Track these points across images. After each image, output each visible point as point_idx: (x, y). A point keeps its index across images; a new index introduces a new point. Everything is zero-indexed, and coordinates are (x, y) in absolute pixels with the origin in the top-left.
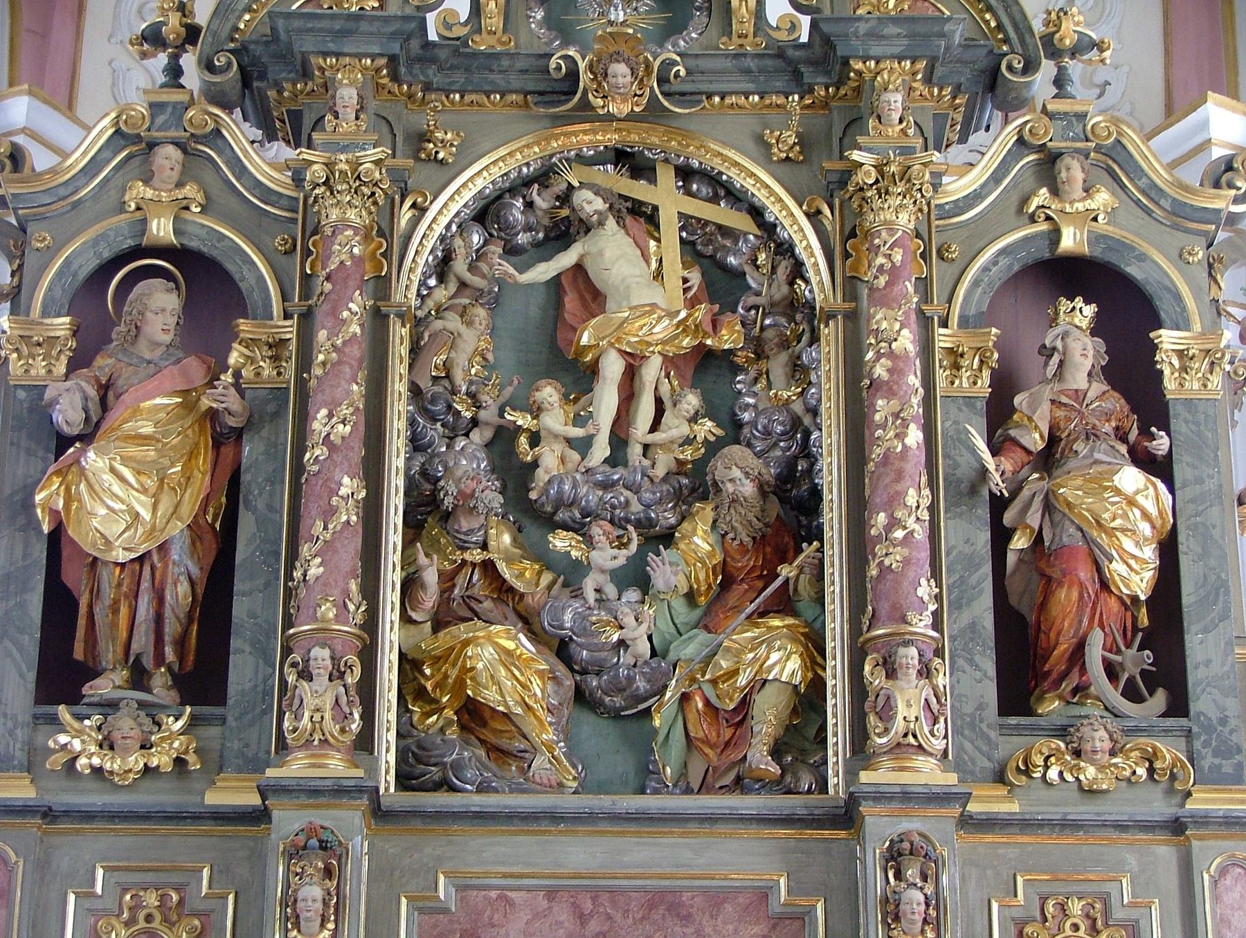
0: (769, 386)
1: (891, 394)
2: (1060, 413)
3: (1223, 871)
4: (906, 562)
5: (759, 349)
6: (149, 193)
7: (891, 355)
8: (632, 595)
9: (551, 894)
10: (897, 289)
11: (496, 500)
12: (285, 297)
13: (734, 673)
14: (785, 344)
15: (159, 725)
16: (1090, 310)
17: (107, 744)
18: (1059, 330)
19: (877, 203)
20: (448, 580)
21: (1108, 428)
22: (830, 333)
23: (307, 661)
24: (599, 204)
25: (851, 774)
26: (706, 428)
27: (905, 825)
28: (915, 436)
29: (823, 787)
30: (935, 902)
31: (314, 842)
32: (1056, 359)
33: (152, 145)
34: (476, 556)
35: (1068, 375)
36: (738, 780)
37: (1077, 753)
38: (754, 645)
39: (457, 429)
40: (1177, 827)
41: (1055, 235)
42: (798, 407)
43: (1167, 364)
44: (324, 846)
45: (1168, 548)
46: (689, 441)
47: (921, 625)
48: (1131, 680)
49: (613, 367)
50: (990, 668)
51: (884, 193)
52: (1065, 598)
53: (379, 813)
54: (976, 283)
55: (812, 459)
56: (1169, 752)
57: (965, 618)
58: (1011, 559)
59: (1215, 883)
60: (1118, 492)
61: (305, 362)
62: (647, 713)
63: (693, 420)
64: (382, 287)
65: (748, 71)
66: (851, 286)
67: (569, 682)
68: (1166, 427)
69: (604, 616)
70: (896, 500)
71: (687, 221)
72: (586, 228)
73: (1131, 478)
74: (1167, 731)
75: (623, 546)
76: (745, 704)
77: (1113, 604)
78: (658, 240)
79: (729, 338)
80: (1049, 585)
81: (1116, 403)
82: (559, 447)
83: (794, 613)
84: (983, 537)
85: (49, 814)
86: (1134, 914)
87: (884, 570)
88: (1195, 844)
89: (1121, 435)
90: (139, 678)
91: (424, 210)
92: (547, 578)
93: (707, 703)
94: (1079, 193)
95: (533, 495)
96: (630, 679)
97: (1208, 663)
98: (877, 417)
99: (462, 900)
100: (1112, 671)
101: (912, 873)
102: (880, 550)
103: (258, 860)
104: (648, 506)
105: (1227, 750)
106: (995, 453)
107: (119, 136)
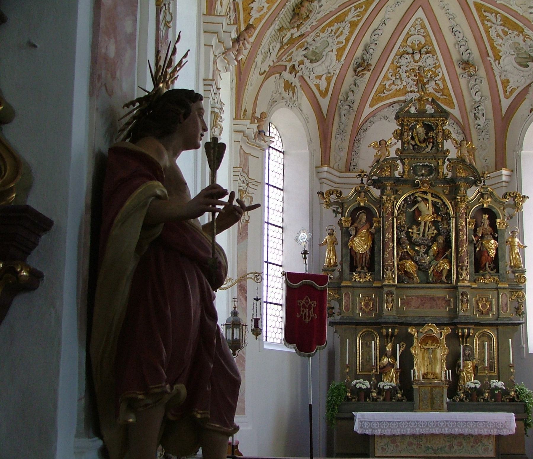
0: (444, 225)
1: (462, 231)
2: (483, 231)
3: (503, 294)
4: (464, 255)
5: (442, 219)
6: (360, 199)
7: (462, 226)
8: (426, 255)
9: (418, 297)
10: (463, 216)
11: (408, 242)
12: (380, 215)
13: (440, 267)
14: (446, 219)
15: (366, 275)
16: (487, 216)
17: (360, 278)
18: (483, 219)
19: (460, 204)
20: (402, 253)
21: (489, 233)
22: (453, 220)
23: (387, 268)
24: (421, 199)
26: (435, 232)
27: (464, 290)
28: (465, 237)
29: (452, 283)
30: (467, 300)
31: (390, 293)
32: (483, 224)
34: (405, 250)
35: (484, 226)
36: (441, 281)
37: (485, 279)
40: (497, 289)
41: (483, 205)
42: (448, 228)
43: (498, 224)
44: (391, 293)
45: (497, 250)
46: (433, 233)
48: (492, 268)
49: (423, 223)
51: (461, 202)
52: (484, 258)
53: (397, 287)
54: (472, 212)
55: (450, 236)
56: (496, 278)
57: (471, 259)
58: (476, 251)
59: (501, 296)
60: (491, 243)
62: (428, 271)
63: (434, 230)
65: (442, 182)
67: (418, 267)
68: (497, 233)
69: (422, 258)
70: (462, 246)
71: (432, 201)
72: (419, 202)
73: (493, 241)
74: (495, 275)
75: (424, 248)
76: (442, 271)
77: (490, 258)
78: (428, 204)
79: (439, 219)
80: (482, 256)
81: (491, 229)
82: (416, 234)
83: (448, 259)
84: (473, 248)
85: (354, 287)
86: (491, 300)
87: (461, 256)
88: (499, 291)
89: (491, 234)
90: (362, 268)
91: (398, 202)
92: (414, 253)
93: (436, 270)
94: (486, 199)
95: (412, 241)
96: (426, 267)
97: (501, 266)
98: (460, 235)
99: (407, 298)
100: (489, 267)
101: (464, 296)
102: (460, 253)
103: (381, 293)
104: (428, 243)
105: (504, 278)
106: (475, 237)
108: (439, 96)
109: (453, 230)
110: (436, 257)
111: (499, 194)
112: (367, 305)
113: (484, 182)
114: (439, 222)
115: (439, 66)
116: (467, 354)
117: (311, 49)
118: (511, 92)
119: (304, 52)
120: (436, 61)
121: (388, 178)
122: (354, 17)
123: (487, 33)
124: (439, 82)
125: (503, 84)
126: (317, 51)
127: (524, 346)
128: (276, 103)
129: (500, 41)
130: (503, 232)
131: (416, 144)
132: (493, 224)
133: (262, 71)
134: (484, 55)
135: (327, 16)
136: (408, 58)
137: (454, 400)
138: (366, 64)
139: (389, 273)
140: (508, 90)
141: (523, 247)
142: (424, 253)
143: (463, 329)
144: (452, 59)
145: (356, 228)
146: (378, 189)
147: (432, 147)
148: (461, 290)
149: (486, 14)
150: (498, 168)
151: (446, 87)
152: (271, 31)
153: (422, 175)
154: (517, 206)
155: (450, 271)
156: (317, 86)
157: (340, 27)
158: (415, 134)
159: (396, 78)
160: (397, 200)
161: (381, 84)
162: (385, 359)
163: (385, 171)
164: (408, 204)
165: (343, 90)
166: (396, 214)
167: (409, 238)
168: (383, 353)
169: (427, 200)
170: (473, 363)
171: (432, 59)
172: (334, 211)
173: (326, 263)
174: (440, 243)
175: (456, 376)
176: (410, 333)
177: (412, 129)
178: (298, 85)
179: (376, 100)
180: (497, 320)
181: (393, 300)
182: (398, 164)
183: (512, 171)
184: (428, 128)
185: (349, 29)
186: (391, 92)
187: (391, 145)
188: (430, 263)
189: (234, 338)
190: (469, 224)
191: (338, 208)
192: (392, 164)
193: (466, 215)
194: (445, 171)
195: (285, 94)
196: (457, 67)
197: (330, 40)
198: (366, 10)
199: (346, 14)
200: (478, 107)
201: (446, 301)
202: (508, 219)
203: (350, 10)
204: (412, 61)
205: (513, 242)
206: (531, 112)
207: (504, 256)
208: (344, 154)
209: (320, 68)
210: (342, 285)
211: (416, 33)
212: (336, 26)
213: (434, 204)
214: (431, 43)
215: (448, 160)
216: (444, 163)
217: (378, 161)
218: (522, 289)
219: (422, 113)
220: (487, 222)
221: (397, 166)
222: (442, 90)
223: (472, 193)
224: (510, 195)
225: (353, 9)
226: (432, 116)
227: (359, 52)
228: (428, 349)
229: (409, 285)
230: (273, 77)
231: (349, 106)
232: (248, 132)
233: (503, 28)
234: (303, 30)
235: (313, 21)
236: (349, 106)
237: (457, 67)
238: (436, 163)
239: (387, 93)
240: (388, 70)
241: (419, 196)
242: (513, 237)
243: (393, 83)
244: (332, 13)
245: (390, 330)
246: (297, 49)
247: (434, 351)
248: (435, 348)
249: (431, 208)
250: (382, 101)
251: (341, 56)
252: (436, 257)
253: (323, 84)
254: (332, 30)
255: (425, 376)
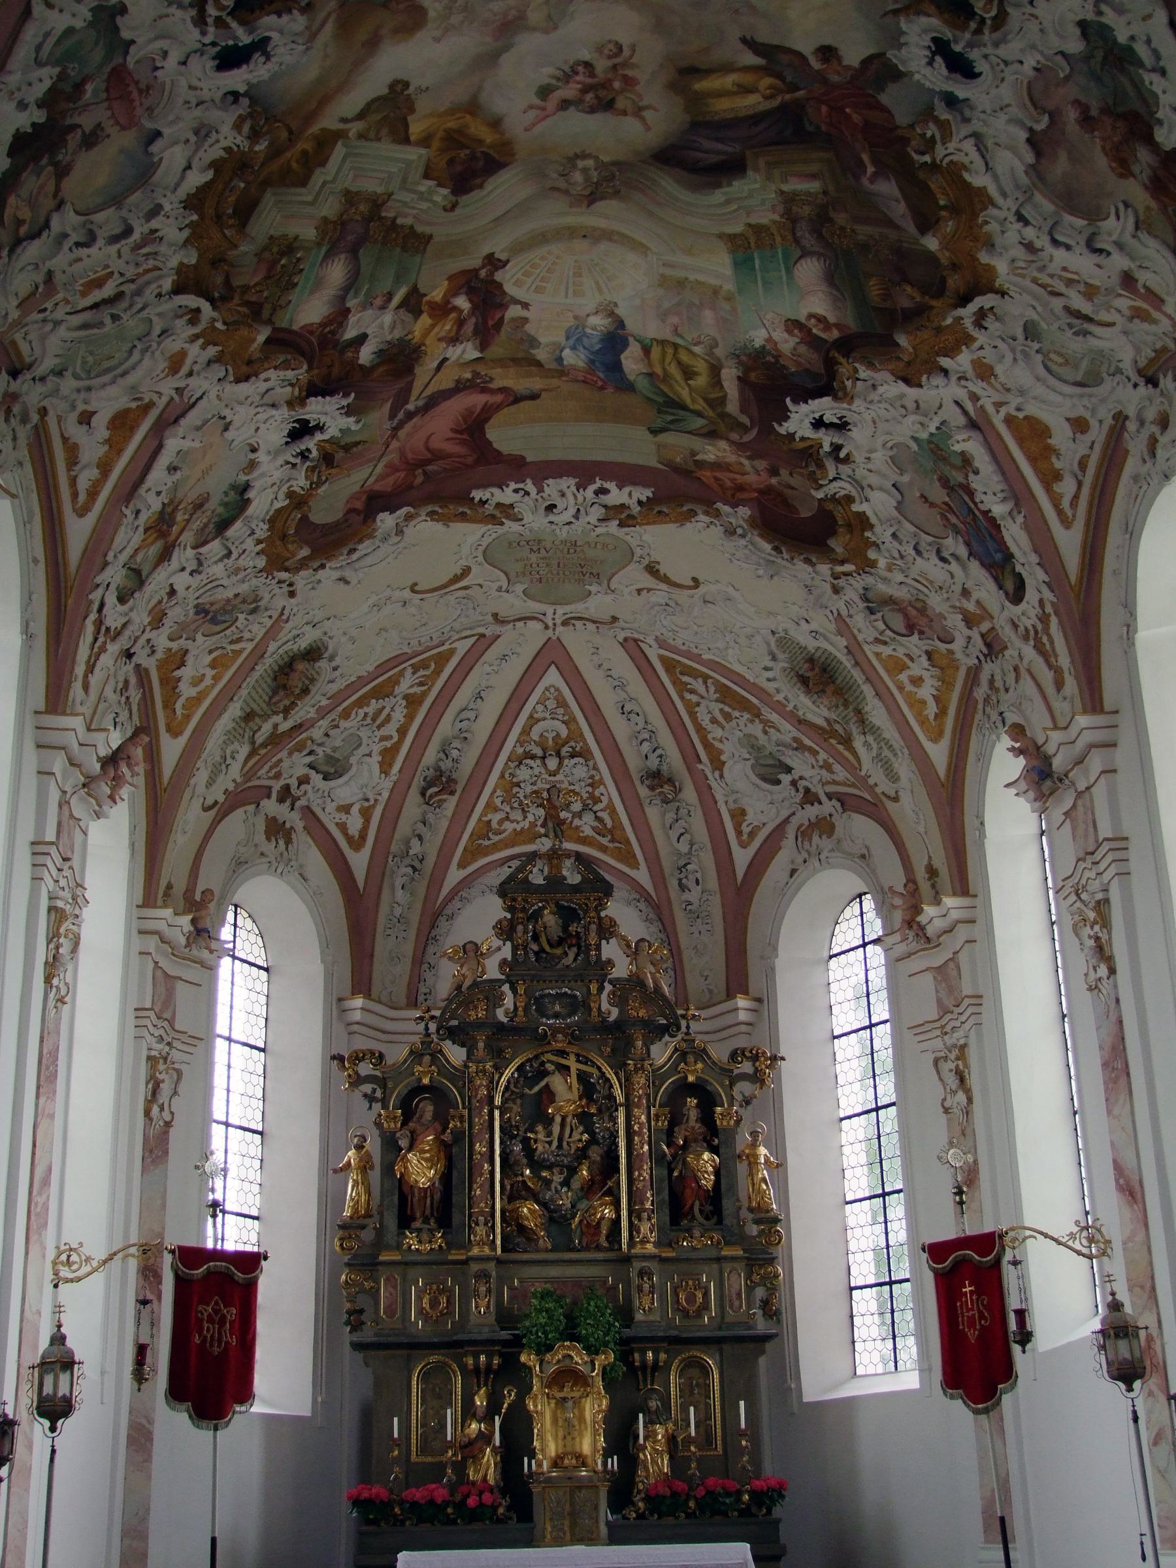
5: (600, 1111)
8: (565, 1189)
11: (525, 1161)
12: (463, 1103)
14: (608, 1109)
17: (420, 1242)
20: (512, 1186)
22: (622, 1110)
25: (629, 1249)
27: (644, 1264)
28: (646, 1147)
30: (652, 1286)
33: (423, 1055)
34: (520, 1178)
38: (601, 1205)
39: (514, 1137)
40: (719, 1259)
41: (686, 1077)
45: (717, 1172)
46: (580, 1140)
47: (648, 1205)
49: (558, 1119)
50: (667, 1211)
52: (688, 1192)
61: (471, 1127)
63: (582, 1134)
64: (491, 1099)
66: (627, 1097)
70: (641, 1168)
73: (706, 1156)
76: (599, 1223)
81: (703, 1129)
84: (665, 1172)
85: (406, 1264)
89: (705, 1140)
90: (426, 1220)
100: (701, 1211)
107: (412, 1052)
108: (606, 844)
109: (622, 1133)
110: (589, 1190)
111: (719, 1052)
112: (434, 1303)
113: (688, 1027)
114: (593, 1115)
115: (601, 782)
116: (654, 1409)
117: (321, 754)
118: (752, 835)
119: (308, 759)
120: (593, 772)
121: (479, 1025)
122: (412, 686)
123: (693, 715)
124: (605, 815)
125: (733, 816)
126: (337, 755)
127: (793, 1386)
128: (246, 866)
129: (717, 732)
130: (731, 1133)
131: (542, 950)
132: (707, 1118)
133: (209, 802)
134: (690, 758)
135: (352, 688)
136: (534, 765)
137: (624, 1518)
138: (444, 779)
139: (481, 1230)
140: (746, 829)
141: (779, 1166)
142: (563, 1184)
143: (643, 1353)
144: (627, 769)
145: (412, 1132)
146: (463, 1045)
147: (577, 955)
148: (637, 1265)
149: (685, 679)
150: (730, 996)
151: (617, 824)
152: (225, 722)
153: (556, 1016)
154: (758, 1078)
155: (617, 1222)
156: (342, 827)
157: (384, 708)
158: (540, 928)
159: (512, 808)
160: (499, 1069)
161: (480, 819)
162: (473, 1426)
163: (476, 1008)
164: (526, 1078)
165: (398, 836)
166: (498, 1101)
167: (529, 1151)
168: (469, 1411)
169: (567, 1068)
170: (667, 1431)
171: (585, 769)
172: (365, 1095)
173: (347, 1213)
174: (594, 1162)
175: (630, 1462)
176: (524, 1365)
177: (536, 916)
178: (299, 825)
179: (472, 853)
180: (720, 1328)
181: (489, 1291)
182: (503, 993)
183: (759, 1000)
184: (568, 915)
185: (405, 711)
186: (504, 835)
187: (491, 952)
188: (573, 1206)
189: (45, 1394)
190: (657, 1120)
191: (374, 1091)
192: (489, 992)
193: (648, 1100)
194: (605, 1006)
195: (269, 848)
196: (637, 783)
197: (364, 733)
198: (438, 672)
199: (395, 681)
200: (686, 865)
201: (609, 1289)
202: (741, 1106)
203: (401, 674)
204: (543, 771)
205: (756, 1156)
206: (791, 876)
207: (733, 1187)
208: (403, 970)
209: (346, 790)
210: (381, 1258)
211: (548, 716)
212: (374, 705)
213: (582, 1077)
214: (582, 735)
215: (610, 982)
216: (601, 989)
217: (459, 987)
218: (774, 1259)
219: (555, 882)
220: (693, 1114)
221: (501, 997)
222: (610, 831)
223: (662, 1053)
224: (743, 1054)
225: (410, 670)
226: (575, 889)
227: (431, 755)
228: (564, 1399)
229: (526, 1257)
230: (239, 812)
231: (413, 867)
232: (168, 932)
233: (721, 706)
234: (298, 716)
235: (319, 697)
236: (413, 867)
237: (637, 783)
238: (585, 989)
239: (495, 838)
240: (494, 791)
241: (549, 1061)
242: (754, 1145)
243: (507, 818)
244: (362, 681)
245: (483, 1358)
246: (290, 754)
247: (577, 1402)
248: (581, 1397)
249: (575, 1085)
250: (486, 855)
251: (391, 765)
252: (589, 1190)
253: (355, 823)
254: (366, 714)
255: (556, 1463)
